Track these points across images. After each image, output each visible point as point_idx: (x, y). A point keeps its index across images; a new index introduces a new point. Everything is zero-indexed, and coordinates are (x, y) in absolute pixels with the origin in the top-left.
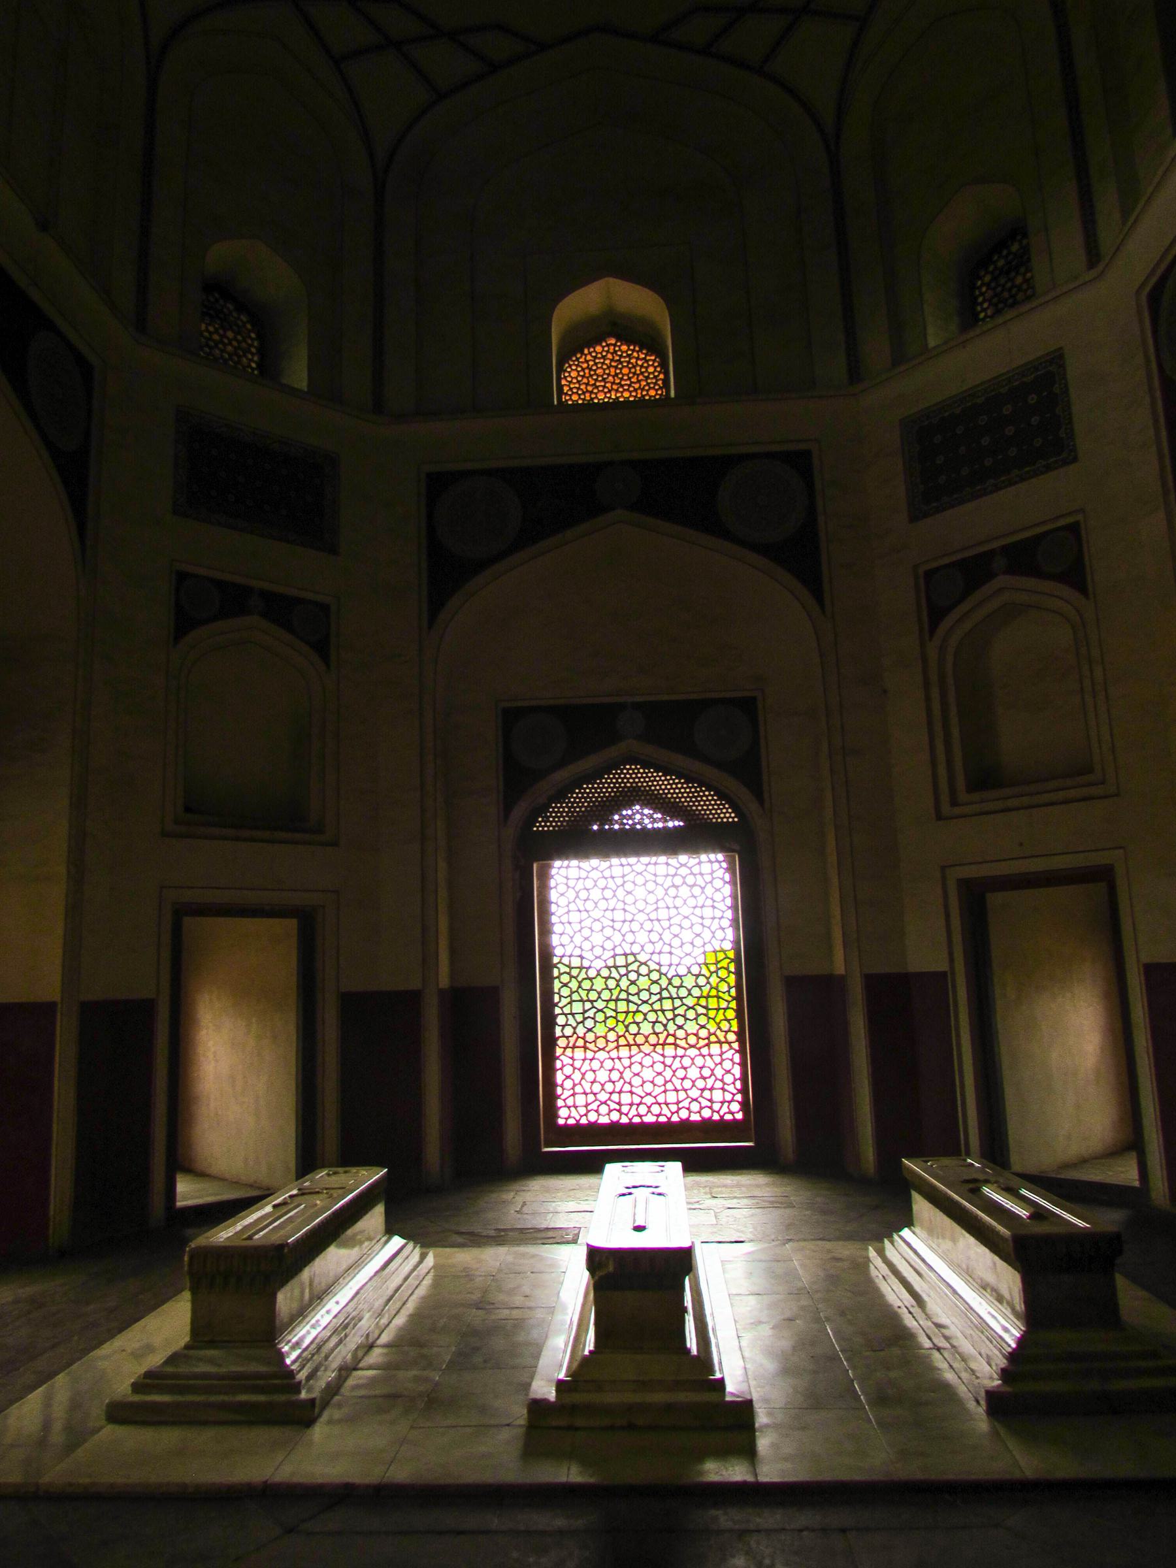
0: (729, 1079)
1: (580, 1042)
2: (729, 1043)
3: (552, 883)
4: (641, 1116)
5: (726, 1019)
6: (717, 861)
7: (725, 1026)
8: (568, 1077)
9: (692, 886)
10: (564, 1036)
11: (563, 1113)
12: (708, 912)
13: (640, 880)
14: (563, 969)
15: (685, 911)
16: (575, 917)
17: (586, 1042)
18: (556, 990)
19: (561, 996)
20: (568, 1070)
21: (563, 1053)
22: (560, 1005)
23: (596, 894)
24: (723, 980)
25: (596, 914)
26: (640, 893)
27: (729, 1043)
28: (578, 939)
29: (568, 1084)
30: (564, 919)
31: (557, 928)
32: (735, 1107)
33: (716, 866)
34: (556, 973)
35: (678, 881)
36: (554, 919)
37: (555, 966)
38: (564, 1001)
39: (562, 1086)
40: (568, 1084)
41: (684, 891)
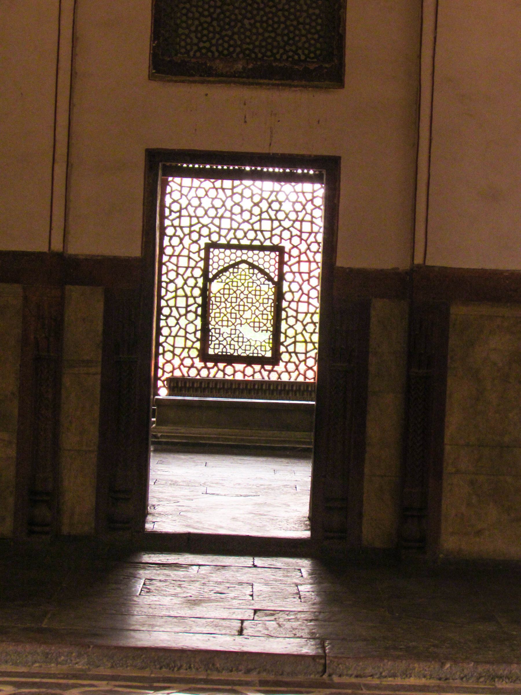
1: (182, 333)
3: (168, 190)
8: (168, 362)
9: (294, 203)
14: (171, 266)
17: (186, 332)
19: (167, 291)
20: (169, 356)
22: (166, 298)
23: (206, 203)
25: (205, 221)
26: (247, 204)
30: (176, 223)
31: (170, 231)
34: (164, 270)
35: (281, 197)
36: (167, 223)
37: (164, 264)
38: (170, 295)
39: (163, 369)
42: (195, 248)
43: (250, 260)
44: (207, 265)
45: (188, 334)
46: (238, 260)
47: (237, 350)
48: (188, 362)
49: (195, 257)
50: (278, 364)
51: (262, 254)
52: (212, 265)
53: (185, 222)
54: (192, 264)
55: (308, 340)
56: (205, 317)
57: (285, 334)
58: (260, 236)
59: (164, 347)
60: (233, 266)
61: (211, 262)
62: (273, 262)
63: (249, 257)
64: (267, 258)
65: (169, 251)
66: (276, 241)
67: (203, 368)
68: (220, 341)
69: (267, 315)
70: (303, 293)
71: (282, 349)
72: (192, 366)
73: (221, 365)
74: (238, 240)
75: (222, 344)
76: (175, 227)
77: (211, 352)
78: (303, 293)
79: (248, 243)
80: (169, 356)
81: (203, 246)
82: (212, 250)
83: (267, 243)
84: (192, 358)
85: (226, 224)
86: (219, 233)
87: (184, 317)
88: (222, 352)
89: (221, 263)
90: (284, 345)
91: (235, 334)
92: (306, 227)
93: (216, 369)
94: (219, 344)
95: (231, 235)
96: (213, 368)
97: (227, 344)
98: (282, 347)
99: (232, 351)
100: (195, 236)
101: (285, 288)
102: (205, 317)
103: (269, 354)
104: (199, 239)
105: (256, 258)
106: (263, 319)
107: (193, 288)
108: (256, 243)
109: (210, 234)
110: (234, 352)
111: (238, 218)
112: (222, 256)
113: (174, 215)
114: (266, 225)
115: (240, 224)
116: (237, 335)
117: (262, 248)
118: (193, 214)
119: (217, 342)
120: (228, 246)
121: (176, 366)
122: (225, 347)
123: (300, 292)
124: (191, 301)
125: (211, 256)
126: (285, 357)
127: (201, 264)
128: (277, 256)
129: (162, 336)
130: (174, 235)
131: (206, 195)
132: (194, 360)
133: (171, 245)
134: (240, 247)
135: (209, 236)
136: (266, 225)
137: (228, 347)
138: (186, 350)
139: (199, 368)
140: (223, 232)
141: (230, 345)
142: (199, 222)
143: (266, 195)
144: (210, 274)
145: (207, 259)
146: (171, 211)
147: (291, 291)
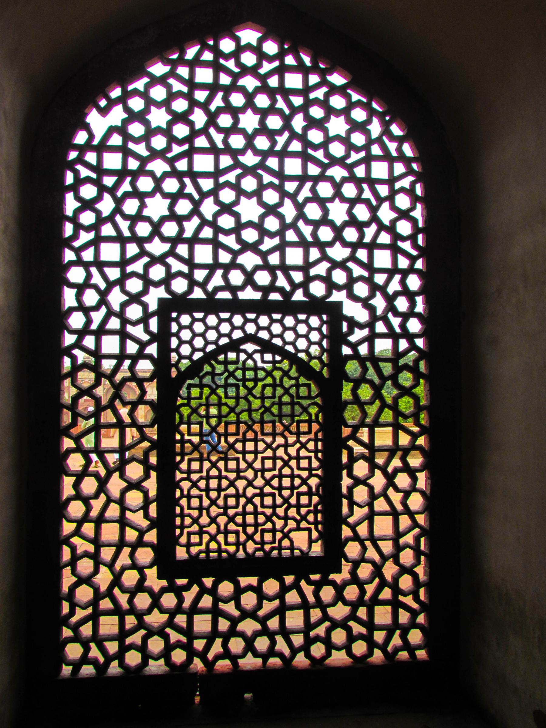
0: (406, 582)
1: (114, 511)
2: (411, 514)
4: (234, 659)
5: (406, 468)
6: (402, 158)
7: (402, 480)
10: (79, 496)
11: (74, 651)
12: (382, 259)
13: (249, 184)
14: (81, 356)
15: (338, 253)
16: (110, 252)
20: (85, 566)
21: (77, 532)
24: (405, 391)
26: (249, 210)
27: (411, 514)
28: (116, 298)
29: (84, 593)
30: (88, 255)
31: (76, 275)
32: (415, 636)
33: (399, 168)
36: (69, 256)
39: (71, 596)
40: (84, 593)
41: (338, 212)
42: (134, 312)
43: (264, 335)
44: (165, 350)
45: (128, 512)
46: (237, 334)
47: (244, 545)
48: (130, 578)
49: (138, 331)
50: (339, 570)
51: (289, 321)
52: (177, 350)
54: (132, 348)
55: (399, 507)
56: (166, 472)
57: (350, 496)
58: (282, 282)
60: (224, 349)
61: (174, 342)
62: (315, 336)
63: (259, 328)
64: (302, 329)
66: (318, 289)
67: (164, 590)
68: (201, 527)
69: (309, 458)
70: (384, 405)
71: (346, 532)
72: (140, 587)
73: (208, 582)
74: (234, 290)
75: (207, 532)
76: (86, 265)
77: (181, 553)
78: (384, 405)
79: (257, 296)
80: (85, 566)
81: (153, 307)
82: (174, 315)
83: (299, 296)
84: (141, 570)
85: (203, 254)
86: (189, 277)
87: (117, 473)
88: (208, 551)
89: (199, 342)
90: (348, 524)
91: (237, 506)
92: (382, 259)
93: (195, 589)
94: (201, 533)
95: (217, 280)
96: (188, 587)
97: (219, 532)
98: (344, 526)
99: (232, 549)
100: (134, 285)
101: (346, 394)
102: (166, 472)
103: (317, 549)
104: (145, 291)
105: (276, 329)
106: (299, 468)
107: (134, 405)
108: (275, 296)
109: (170, 276)
110: (238, 550)
111: (230, 241)
112: (199, 327)
114: (294, 256)
115: (235, 254)
116: (240, 509)
117: (287, 307)
118: (127, 233)
119: (195, 528)
120: (211, 305)
121: (103, 588)
122: (213, 538)
123: (377, 403)
124: (131, 434)
125: (174, 328)
126: (352, 550)
127: (152, 349)
128: (323, 322)
129: (69, 521)
130: (87, 285)
131: (158, 189)
132: (145, 570)
134: (237, 306)
135: (166, 282)
136: (294, 256)
137: (221, 538)
138: (126, 551)
139: (156, 589)
140: (200, 275)
141: (226, 533)
142: (143, 253)
143: (290, 187)
144: (174, 370)
145: (162, 337)
147: (356, 400)
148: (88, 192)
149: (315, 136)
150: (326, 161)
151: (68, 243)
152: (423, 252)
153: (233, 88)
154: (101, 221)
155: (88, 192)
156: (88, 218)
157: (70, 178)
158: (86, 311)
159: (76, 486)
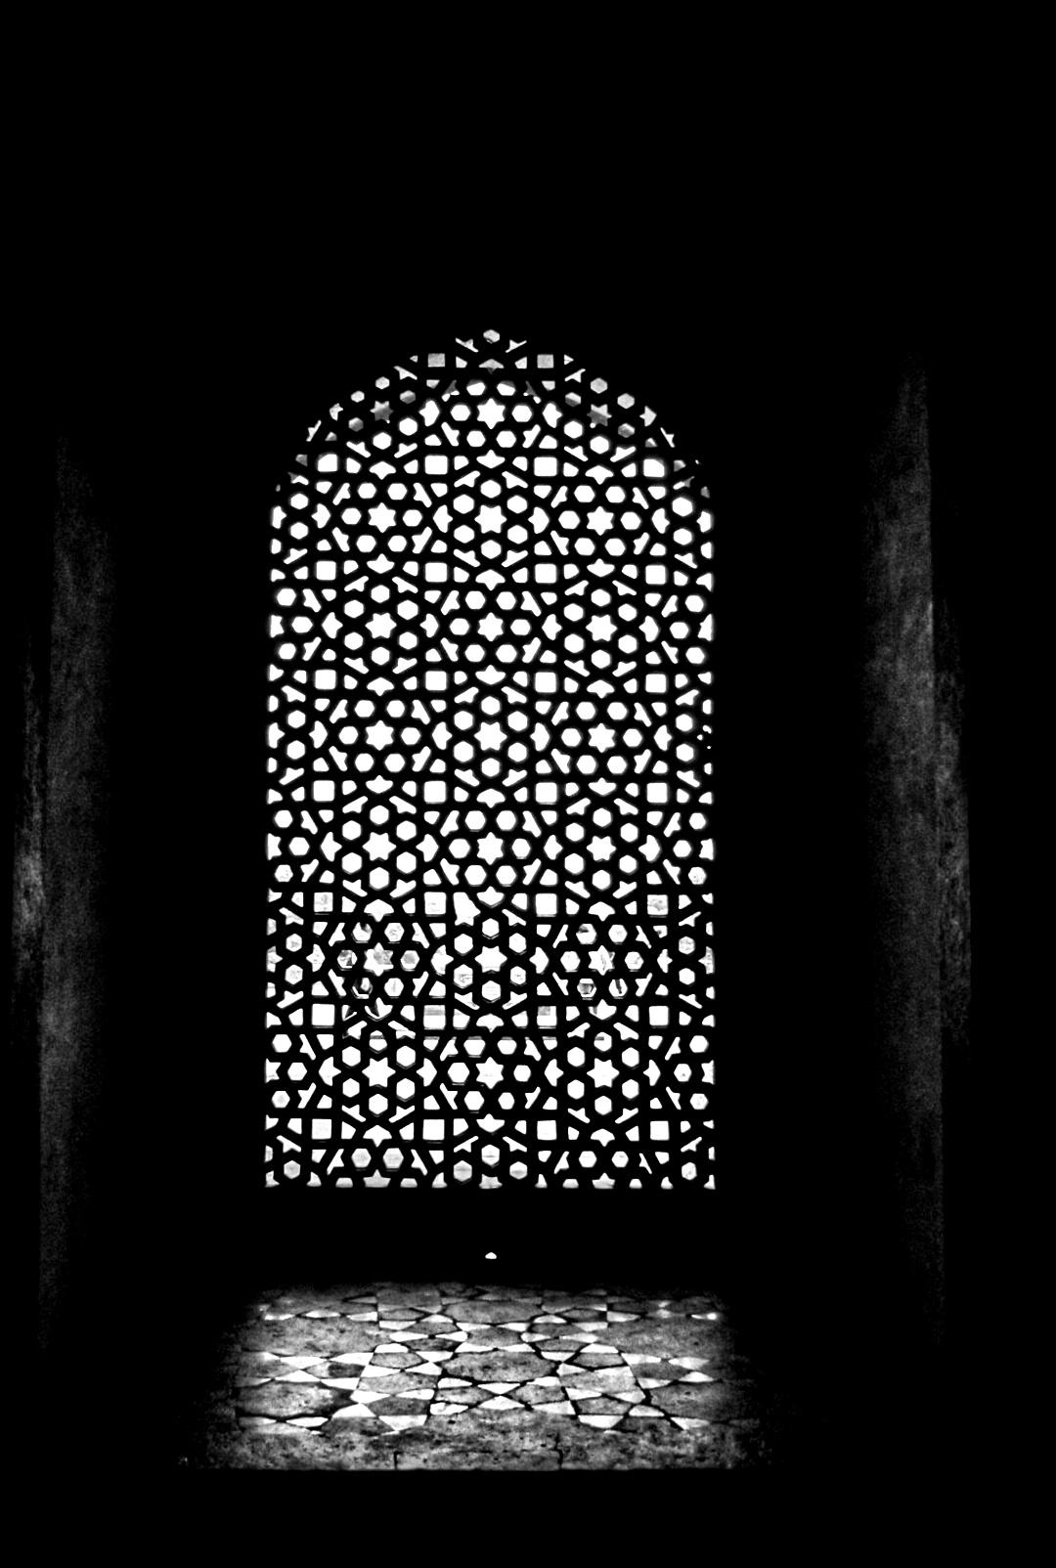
5: (686, 1056)
14: (291, 918)
18: (271, 968)
36: (274, 796)
53: (324, 791)
59: (278, 1147)
65: (284, 874)
113: (292, 775)
133: (287, 857)
143: (543, 707)
146: (285, 763)
148: (297, 719)
149: (574, 643)
150: (586, 673)
151: (273, 781)
152: (707, 783)
153: (472, 585)
154: (312, 753)
155: (297, 719)
156: (296, 750)
157: (273, 703)
158: (296, 863)
159: (282, 1072)
